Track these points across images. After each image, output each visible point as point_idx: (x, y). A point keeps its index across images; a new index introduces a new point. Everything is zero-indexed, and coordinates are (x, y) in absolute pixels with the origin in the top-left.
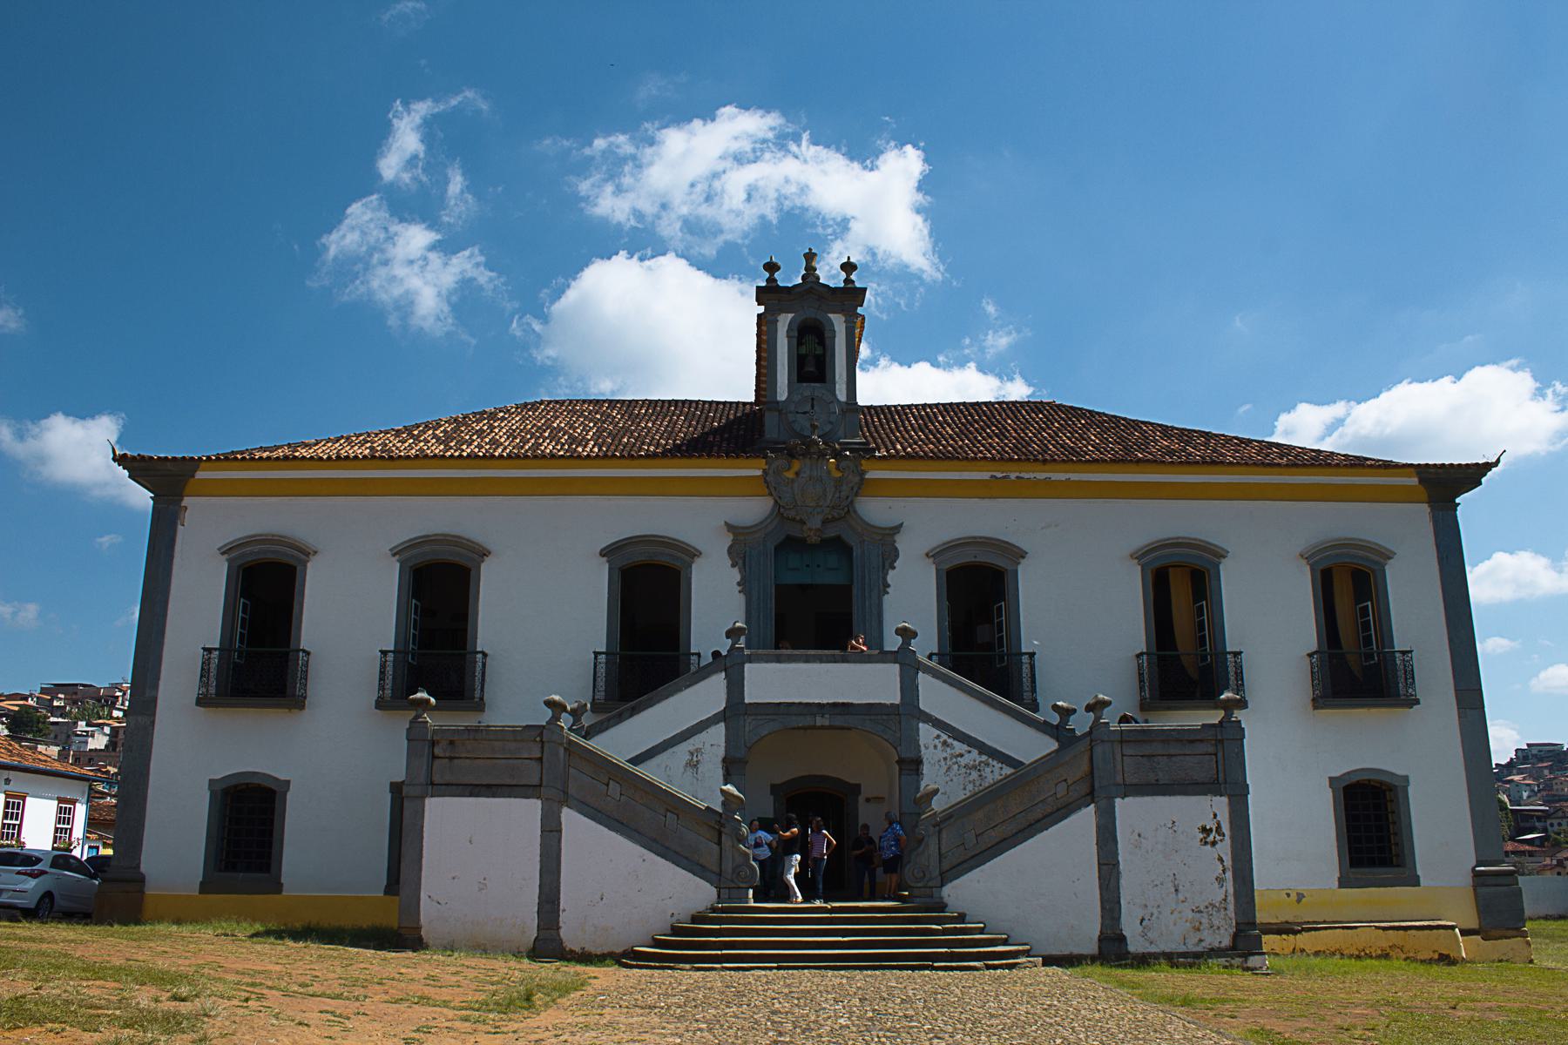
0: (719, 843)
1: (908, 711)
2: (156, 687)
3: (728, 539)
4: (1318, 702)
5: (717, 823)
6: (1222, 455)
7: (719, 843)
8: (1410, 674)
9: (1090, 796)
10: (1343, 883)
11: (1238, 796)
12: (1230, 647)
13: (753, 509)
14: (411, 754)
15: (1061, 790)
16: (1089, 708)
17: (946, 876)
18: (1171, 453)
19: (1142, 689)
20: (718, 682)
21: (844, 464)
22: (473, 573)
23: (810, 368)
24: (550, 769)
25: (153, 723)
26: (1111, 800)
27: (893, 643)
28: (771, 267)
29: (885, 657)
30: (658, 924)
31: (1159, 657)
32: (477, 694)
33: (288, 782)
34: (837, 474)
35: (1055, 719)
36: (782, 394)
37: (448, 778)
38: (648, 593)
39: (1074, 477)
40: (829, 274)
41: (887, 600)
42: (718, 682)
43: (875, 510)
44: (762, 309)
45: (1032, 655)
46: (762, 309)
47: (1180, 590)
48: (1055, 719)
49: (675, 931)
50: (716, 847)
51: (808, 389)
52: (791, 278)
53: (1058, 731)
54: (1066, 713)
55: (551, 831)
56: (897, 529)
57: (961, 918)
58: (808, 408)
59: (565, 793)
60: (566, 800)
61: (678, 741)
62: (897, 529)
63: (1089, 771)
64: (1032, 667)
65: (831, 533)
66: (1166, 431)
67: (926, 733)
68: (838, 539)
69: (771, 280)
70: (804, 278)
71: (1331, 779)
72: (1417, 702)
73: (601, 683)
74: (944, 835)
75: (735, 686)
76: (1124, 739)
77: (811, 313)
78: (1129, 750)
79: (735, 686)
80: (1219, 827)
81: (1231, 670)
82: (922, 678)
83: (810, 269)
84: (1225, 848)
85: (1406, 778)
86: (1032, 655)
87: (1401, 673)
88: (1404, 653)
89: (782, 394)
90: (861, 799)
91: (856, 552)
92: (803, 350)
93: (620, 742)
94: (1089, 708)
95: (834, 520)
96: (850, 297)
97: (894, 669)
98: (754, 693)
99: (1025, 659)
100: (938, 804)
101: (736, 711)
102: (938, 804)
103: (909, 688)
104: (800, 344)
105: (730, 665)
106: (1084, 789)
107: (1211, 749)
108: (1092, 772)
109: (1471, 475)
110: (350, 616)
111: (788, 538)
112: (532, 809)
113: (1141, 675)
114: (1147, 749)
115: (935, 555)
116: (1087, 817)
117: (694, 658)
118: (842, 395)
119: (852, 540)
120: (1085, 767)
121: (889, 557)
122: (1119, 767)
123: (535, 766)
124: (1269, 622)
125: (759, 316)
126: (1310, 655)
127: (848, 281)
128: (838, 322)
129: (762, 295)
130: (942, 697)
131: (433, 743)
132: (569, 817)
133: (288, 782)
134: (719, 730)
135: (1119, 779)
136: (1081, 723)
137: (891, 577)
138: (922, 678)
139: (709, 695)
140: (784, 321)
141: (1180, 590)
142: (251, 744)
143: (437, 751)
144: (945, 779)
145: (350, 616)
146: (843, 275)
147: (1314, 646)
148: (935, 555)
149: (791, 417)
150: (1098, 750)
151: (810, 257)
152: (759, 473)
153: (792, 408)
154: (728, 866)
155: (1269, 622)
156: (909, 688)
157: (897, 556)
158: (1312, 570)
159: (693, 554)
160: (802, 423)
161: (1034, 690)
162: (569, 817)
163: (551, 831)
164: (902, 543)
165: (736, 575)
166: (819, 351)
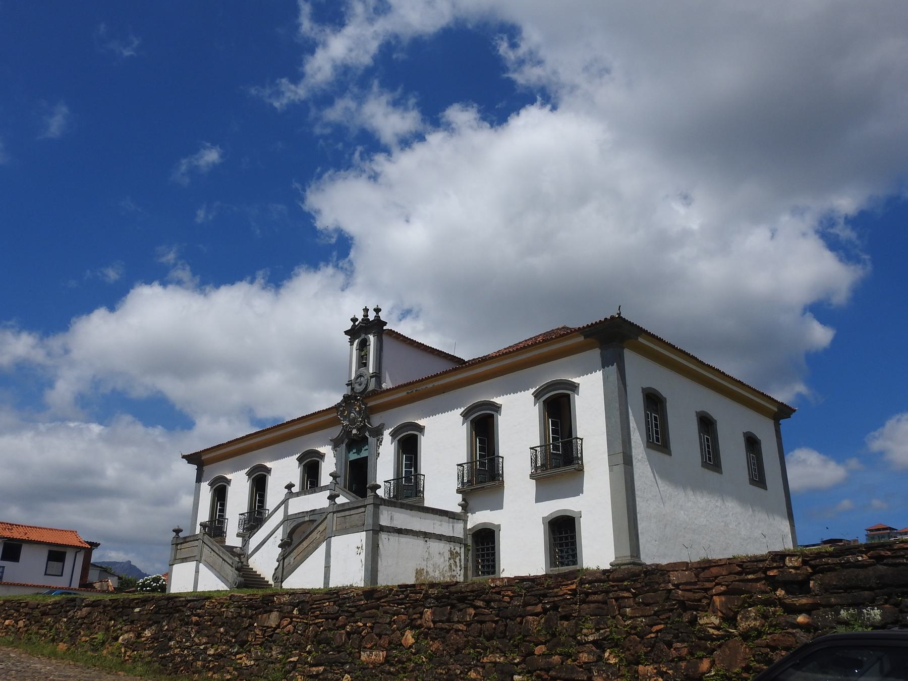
13: (336, 432)
39: (436, 384)
40: (372, 316)
55: (197, 572)
60: (199, 561)
69: (354, 326)
77: (363, 336)
78: (339, 515)
98: (291, 511)
101: (287, 518)
127: (377, 317)
128: (372, 338)
132: (201, 565)
137: (381, 450)
148: (393, 435)
162: (201, 565)
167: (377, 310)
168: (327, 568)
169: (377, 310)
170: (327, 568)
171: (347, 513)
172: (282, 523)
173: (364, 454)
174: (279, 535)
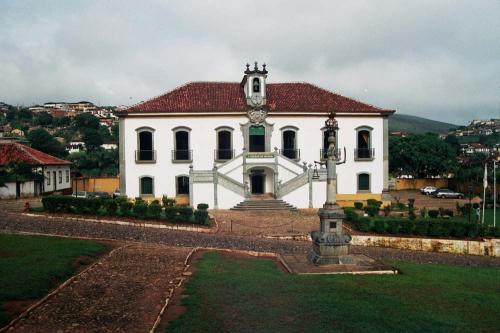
1: (276, 164)
24: (215, 177)
28: (248, 66)
38: (224, 138)
42: (241, 158)
51: (256, 94)
52: (252, 69)
53: (305, 169)
55: (216, 188)
96: (264, 73)
101: (244, 164)
110: (164, 144)
112: (212, 185)
115: (281, 129)
116: (308, 185)
124: (347, 139)
128: (261, 78)
130: (283, 161)
142: (146, 170)
144: (283, 176)
145: (164, 144)
151: (256, 64)
155: (347, 139)
162: (218, 186)
163: (216, 188)
167: (264, 66)
169: (264, 66)
174: (241, 170)
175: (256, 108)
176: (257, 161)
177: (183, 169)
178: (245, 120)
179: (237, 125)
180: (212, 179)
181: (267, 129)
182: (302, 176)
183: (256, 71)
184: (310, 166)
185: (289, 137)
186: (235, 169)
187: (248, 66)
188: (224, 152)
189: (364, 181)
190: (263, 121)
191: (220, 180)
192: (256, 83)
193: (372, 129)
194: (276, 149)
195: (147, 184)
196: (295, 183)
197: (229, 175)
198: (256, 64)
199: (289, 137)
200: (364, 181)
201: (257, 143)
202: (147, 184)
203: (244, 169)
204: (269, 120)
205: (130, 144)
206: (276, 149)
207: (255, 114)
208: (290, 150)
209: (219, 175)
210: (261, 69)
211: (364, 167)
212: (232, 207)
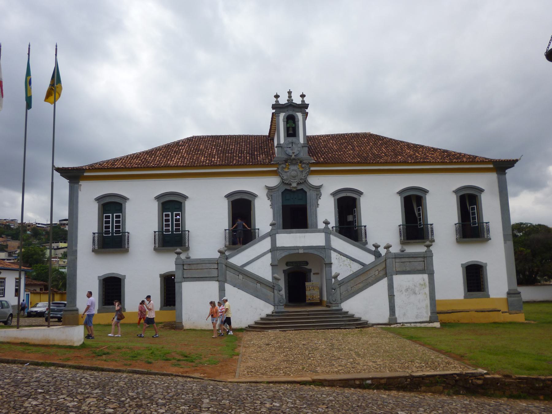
0: (274, 292)
1: (327, 248)
2: (76, 246)
3: (266, 191)
4: (458, 241)
5: (272, 287)
6: (427, 156)
7: (274, 292)
8: (488, 230)
9: (386, 275)
10: (465, 297)
11: (431, 274)
12: (430, 222)
13: (273, 181)
14: (176, 268)
15: (377, 273)
16: (385, 248)
17: (342, 301)
18: (410, 156)
19: (400, 236)
20: (269, 239)
21: (303, 166)
22: (183, 204)
23: (291, 132)
24: (220, 271)
25: (76, 258)
26: (392, 275)
27: (321, 226)
28: (277, 96)
29: (320, 231)
30: (257, 318)
31: (407, 226)
32: (187, 244)
33: (125, 276)
34: (301, 169)
35: (373, 249)
36: (282, 141)
37: (189, 276)
38: (241, 208)
41: (319, 210)
42: (269, 239)
43: (314, 180)
44: (274, 111)
45: (365, 226)
46: (274, 111)
47: (413, 203)
48: (373, 249)
49: (262, 319)
50: (272, 294)
51: (291, 139)
52: (283, 100)
54: (377, 246)
55: (222, 290)
56: (320, 187)
57: (347, 312)
58: (291, 146)
59: (226, 279)
60: (226, 281)
61: (258, 260)
62: (321, 186)
63: (384, 267)
64: (365, 230)
65: (299, 187)
66: (408, 145)
67: (334, 255)
68: (302, 189)
69: (277, 101)
70: (288, 101)
71: (462, 265)
72: (490, 239)
73: (227, 240)
74: (341, 287)
75: (274, 242)
76: (396, 257)
77: (291, 113)
78: (397, 260)
79: (274, 242)
80: (425, 284)
81: (430, 230)
82: (332, 237)
83: (290, 97)
84: (427, 290)
85: (486, 264)
86: (365, 226)
87: (485, 230)
88: (486, 223)
89: (282, 141)
90: (312, 274)
91: (308, 194)
92: (288, 126)
93: (238, 260)
94: (385, 248)
95: (301, 183)
96: (303, 107)
97: (323, 235)
98: (279, 244)
99: (363, 228)
100: (340, 278)
101: (274, 249)
102: (340, 278)
103: (328, 240)
104: (287, 123)
105: (272, 235)
106: (382, 273)
107: (422, 260)
108: (386, 268)
109: (511, 163)
110: (142, 221)
111: (286, 190)
113: (400, 232)
114: (403, 260)
115: (334, 194)
116: (384, 282)
117: (257, 231)
118: (302, 140)
119: (306, 189)
120: (384, 266)
121: (319, 196)
122: (413, 325)
123: (216, 271)
124: (442, 213)
125: (273, 113)
126: (455, 224)
127: (303, 101)
128: (300, 116)
129: (274, 107)
130: (339, 243)
131: (183, 265)
132: (228, 287)
133: (125, 276)
134: (269, 255)
135: (394, 269)
136: (383, 251)
137: (320, 202)
138: (332, 237)
139: (266, 244)
140: (282, 116)
141: (413, 203)
143: (185, 268)
145: (142, 221)
146: (301, 99)
147: (457, 222)
149: (285, 149)
150: (388, 261)
151: (290, 93)
152: (276, 169)
153: (286, 146)
154: (277, 300)
155: (442, 213)
156: (328, 240)
157: (321, 195)
158: (457, 196)
159: (255, 196)
160: (290, 152)
161: (366, 237)
162: (228, 287)
163: (222, 290)
164: (323, 191)
165: (269, 203)
166: (294, 126)
167: (303, 96)
168: (391, 297)
169: (303, 96)
170: (391, 297)
171: (407, 260)
172: (271, 251)
173: (301, 203)
175: (290, 161)
176: (291, 240)
177: (167, 263)
178: (273, 181)
179: (259, 187)
180: (215, 273)
181: (310, 194)
182: (373, 266)
183: (290, 105)
184: (388, 247)
185: (347, 205)
186: (258, 260)
187: (277, 96)
188: (241, 229)
189: (475, 277)
190: (305, 182)
191: (230, 275)
192: (291, 124)
193: (481, 191)
194: (327, 223)
195: (112, 288)
196: (362, 279)
197: (247, 268)
198: (290, 93)
199: (347, 205)
200: (475, 277)
201: (295, 215)
202: (112, 288)
203: (272, 258)
204: (314, 180)
205: (88, 224)
206: (327, 223)
207: (293, 170)
208: (348, 223)
209: (233, 268)
210: (297, 100)
211: (474, 254)
212: (251, 322)
